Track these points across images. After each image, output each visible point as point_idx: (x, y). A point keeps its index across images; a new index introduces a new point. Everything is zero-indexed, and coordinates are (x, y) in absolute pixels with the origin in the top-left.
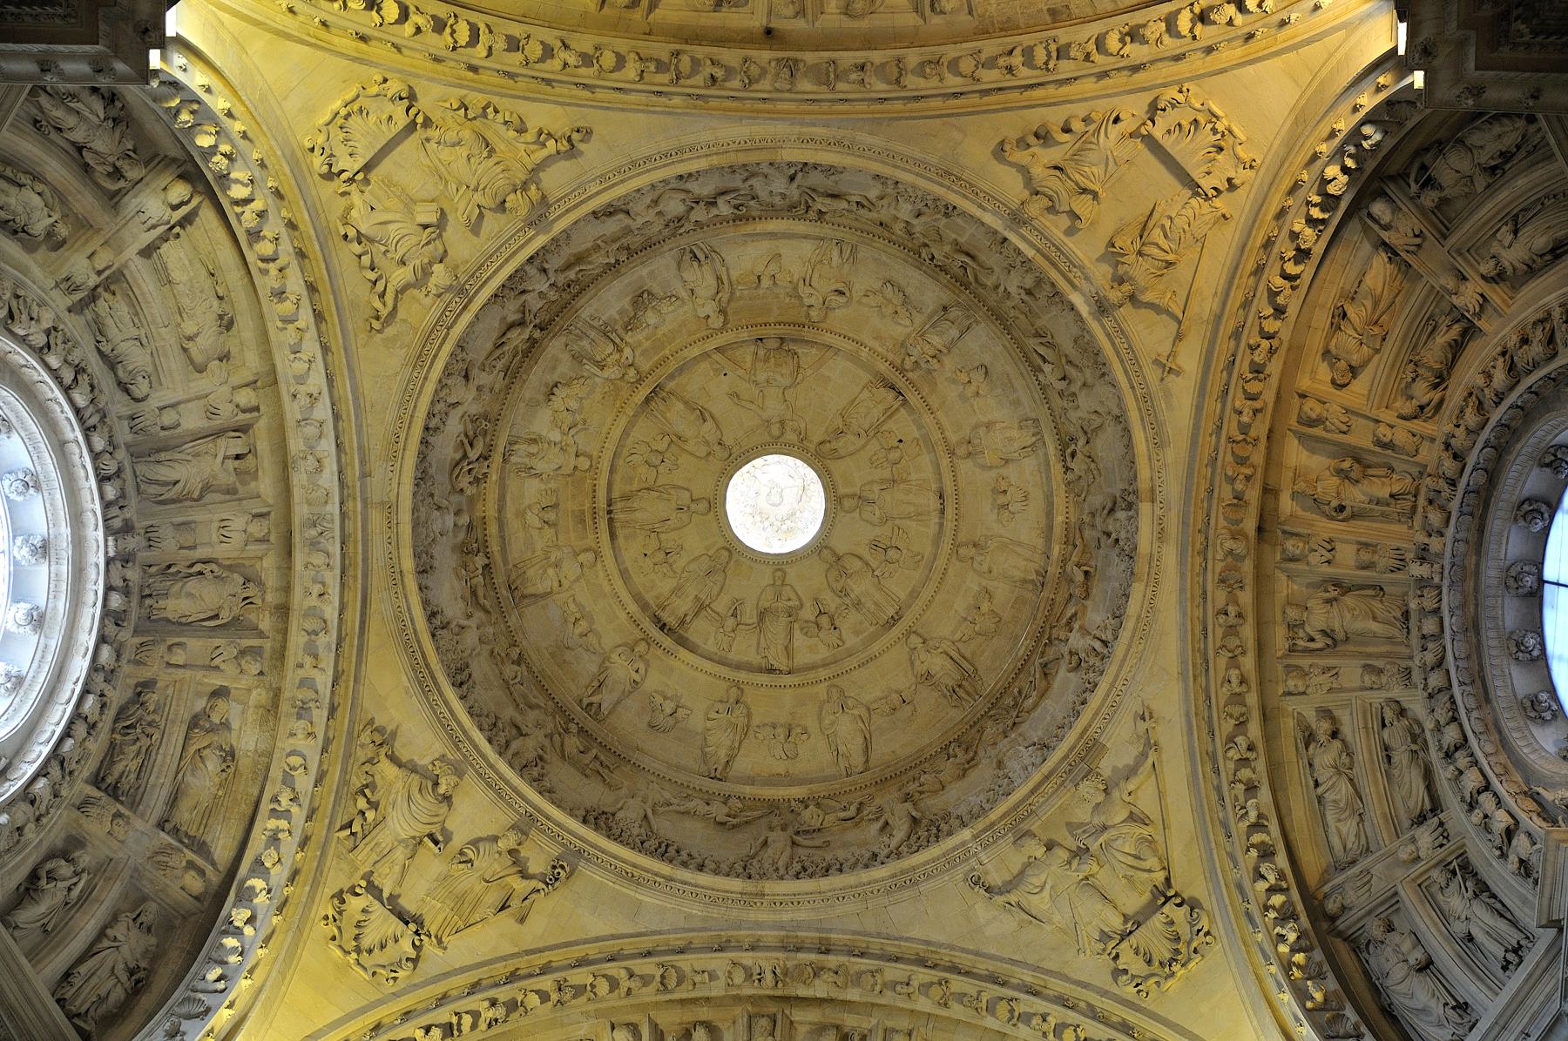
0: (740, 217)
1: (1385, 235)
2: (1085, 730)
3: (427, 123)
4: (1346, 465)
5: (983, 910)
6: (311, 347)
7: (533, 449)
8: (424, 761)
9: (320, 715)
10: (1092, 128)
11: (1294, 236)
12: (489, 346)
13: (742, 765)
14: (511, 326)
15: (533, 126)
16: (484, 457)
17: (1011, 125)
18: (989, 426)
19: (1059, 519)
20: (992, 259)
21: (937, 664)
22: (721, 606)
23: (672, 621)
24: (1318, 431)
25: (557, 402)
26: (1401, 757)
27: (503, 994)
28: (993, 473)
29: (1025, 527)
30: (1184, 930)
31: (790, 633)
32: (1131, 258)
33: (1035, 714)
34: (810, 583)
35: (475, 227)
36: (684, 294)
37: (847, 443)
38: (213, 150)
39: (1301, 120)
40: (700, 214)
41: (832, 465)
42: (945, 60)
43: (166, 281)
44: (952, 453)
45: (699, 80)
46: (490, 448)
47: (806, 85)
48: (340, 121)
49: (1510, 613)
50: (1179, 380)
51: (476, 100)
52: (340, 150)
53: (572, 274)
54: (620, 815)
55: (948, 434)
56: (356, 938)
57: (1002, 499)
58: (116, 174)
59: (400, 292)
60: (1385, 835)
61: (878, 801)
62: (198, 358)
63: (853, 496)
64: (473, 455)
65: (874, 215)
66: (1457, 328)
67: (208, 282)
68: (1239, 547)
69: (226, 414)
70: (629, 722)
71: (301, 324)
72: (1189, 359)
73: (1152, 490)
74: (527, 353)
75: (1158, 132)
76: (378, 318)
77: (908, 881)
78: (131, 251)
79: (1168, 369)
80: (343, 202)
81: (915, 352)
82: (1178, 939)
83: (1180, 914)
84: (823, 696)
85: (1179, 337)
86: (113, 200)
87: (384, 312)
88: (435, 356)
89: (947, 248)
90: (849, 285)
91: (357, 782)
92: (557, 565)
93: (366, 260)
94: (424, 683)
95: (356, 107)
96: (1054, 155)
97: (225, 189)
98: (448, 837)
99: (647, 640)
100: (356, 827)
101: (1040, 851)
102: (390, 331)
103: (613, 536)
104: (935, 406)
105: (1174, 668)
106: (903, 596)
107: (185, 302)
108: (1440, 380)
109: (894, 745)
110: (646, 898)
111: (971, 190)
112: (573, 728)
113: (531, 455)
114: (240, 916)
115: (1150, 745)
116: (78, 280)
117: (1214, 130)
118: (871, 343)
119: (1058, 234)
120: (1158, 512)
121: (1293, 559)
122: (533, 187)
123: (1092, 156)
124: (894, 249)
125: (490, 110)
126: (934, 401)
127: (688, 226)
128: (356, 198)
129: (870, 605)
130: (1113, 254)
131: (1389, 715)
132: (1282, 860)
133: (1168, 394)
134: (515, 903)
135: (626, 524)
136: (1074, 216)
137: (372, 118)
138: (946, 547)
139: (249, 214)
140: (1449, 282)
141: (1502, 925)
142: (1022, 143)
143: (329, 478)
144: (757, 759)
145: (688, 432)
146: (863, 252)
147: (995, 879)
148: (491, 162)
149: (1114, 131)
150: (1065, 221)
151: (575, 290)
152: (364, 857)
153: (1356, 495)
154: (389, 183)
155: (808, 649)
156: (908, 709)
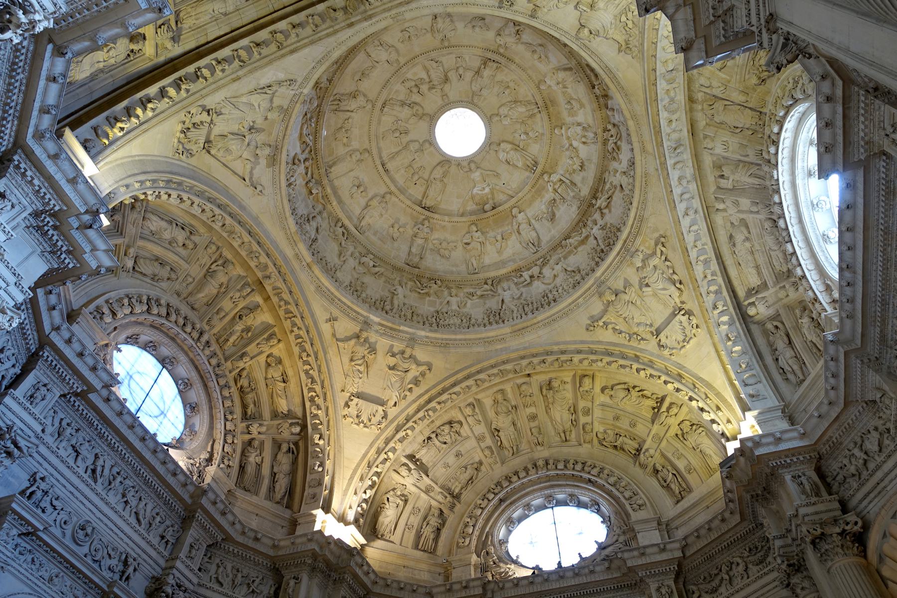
1: (290, 421)
3: (652, 333)
4: (250, 334)
5: (281, 76)
6: (689, 239)
10: (402, 395)
11: (319, 408)
12: (614, 198)
14: (607, 207)
15: (610, 331)
17: (431, 380)
19: (335, 203)
20: (413, 299)
21: (353, 105)
22: (469, 75)
23: (490, 64)
24: (265, 336)
28: (370, 195)
31: (429, 77)
32: (366, 352)
34: (431, 101)
35: (627, 284)
36: (533, 221)
37: (438, 172)
38: (735, 344)
39: (339, 448)
40: (535, 270)
41: (441, 158)
43: (757, 267)
48: (687, 340)
49: (165, 351)
50: (325, 318)
51: (634, 343)
52: (685, 324)
53: (585, 232)
55: (397, 200)
57: (362, 189)
58: (777, 327)
59: (654, 253)
62: (743, 229)
65: (465, 290)
66: (249, 413)
71: (695, 250)
72: (326, 328)
73: (310, 268)
74: (597, 191)
75: (380, 408)
76: (662, 243)
79: (332, 319)
80: (684, 298)
81: (426, 230)
85: (334, 335)
86: (776, 317)
87: (660, 246)
88: (635, 219)
89: (432, 291)
90: (465, 248)
96: (410, 376)
97: (731, 318)
99: (501, 54)
102: (656, 235)
106: (383, 118)
107: (750, 258)
108: (241, 390)
111: (434, 343)
113: (585, 136)
117: (363, 422)
120: (304, 263)
121: (245, 284)
123: (398, 385)
124: (452, 278)
126: (409, 210)
127: (539, 263)
128: (678, 301)
129: (398, 108)
130: (373, 350)
131: (173, 276)
133: (326, 310)
135: (529, 103)
136: (393, 355)
137: (674, 338)
138: (375, 152)
139: (721, 308)
140: (264, 429)
142: (423, 374)
143: (674, 175)
146: (463, 268)
147: (282, 90)
150: (396, 350)
151: (581, 222)
153: (239, 327)
154: (665, 305)
155: (417, 72)
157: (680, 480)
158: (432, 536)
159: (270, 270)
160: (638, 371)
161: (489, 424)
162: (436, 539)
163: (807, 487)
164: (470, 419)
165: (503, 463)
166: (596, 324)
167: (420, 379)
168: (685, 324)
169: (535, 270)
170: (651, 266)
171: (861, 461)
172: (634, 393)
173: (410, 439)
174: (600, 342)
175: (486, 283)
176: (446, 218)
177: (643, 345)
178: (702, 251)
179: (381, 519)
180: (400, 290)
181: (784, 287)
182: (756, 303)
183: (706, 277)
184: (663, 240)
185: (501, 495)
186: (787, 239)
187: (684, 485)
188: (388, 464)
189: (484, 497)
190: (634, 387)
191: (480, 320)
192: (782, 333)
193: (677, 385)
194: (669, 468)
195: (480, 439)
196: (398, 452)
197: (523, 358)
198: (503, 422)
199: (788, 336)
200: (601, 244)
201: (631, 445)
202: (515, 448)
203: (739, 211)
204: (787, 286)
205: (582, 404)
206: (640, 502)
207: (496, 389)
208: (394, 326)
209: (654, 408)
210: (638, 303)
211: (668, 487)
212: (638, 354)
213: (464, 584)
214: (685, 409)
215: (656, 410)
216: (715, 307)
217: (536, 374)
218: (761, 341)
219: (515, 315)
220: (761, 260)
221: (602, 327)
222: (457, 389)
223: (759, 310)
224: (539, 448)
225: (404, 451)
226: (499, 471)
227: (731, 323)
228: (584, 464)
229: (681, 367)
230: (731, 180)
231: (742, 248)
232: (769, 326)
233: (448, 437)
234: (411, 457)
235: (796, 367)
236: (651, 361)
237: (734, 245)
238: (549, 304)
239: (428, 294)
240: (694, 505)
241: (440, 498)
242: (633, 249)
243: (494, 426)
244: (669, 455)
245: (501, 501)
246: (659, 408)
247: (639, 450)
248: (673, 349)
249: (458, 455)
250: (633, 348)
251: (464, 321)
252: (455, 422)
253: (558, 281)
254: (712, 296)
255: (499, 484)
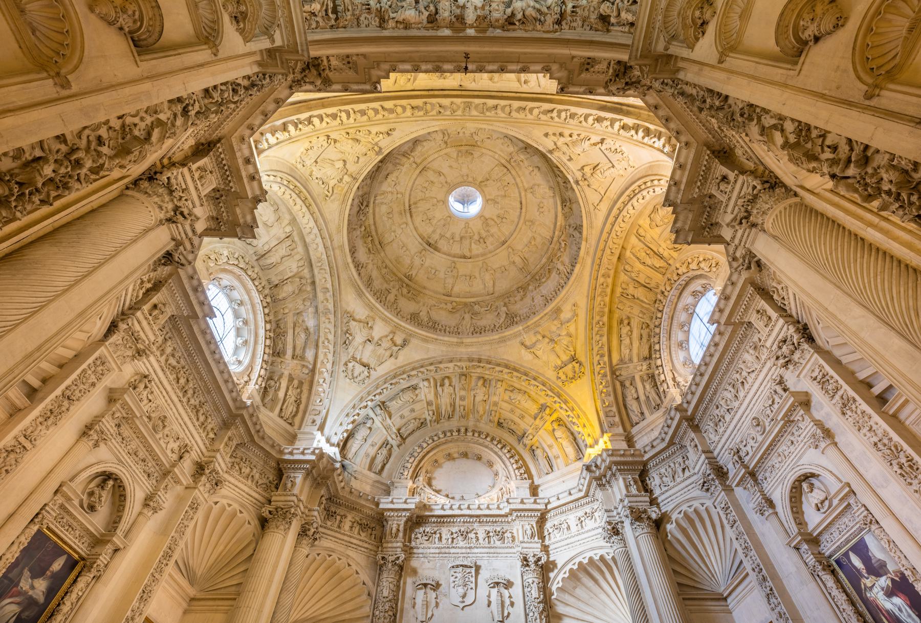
2: (558, 303)
5: (523, 351)
7: (383, 197)
8: (363, 318)
9: (332, 317)
13: (456, 289)
16: (367, 206)
18: (539, 185)
19: (558, 224)
21: (518, 260)
25: (389, 180)
26: (644, 340)
27: (394, 381)
29: (548, 219)
30: (577, 369)
33: (545, 284)
34: (477, 227)
42: (528, 108)
44: (526, 191)
45: (434, 113)
46: (368, 202)
47: (474, 113)
54: (421, 314)
55: (525, 184)
56: (352, 374)
60: (635, 359)
61: (497, 304)
63: (492, 200)
64: (363, 208)
68: (610, 267)
69: (284, 236)
70: (421, 277)
77: (503, 340)
82: (575, 372)
83: (577, 366)
84: (481, 265)
87: (329, 195)
91: (345, 329)
92: (394, 232)
94: (360, 294)
98: (373, 339)
100: (347, 342)
101: (541, 338)
103: (411, 216)
104: (521, 174)
105: (586, 294)
106: (507, 233)
109: (503, 285)
110: (431, 346)
112: (404, 285)
114: (321, 381)
115: (576, 315)
118: (499, 153)
132: (606, 359)
133: (596, 215)
134: (394, 354)
141: (657, 398)
143: (321, 248)
144: (460, 287)
145: (435, 180)
147: (528, 343)
149: (587, 143)
152: (351, 350)
156: (507, 273)
159: (603, 271)
167: (558, 134)
176: (497, 156)
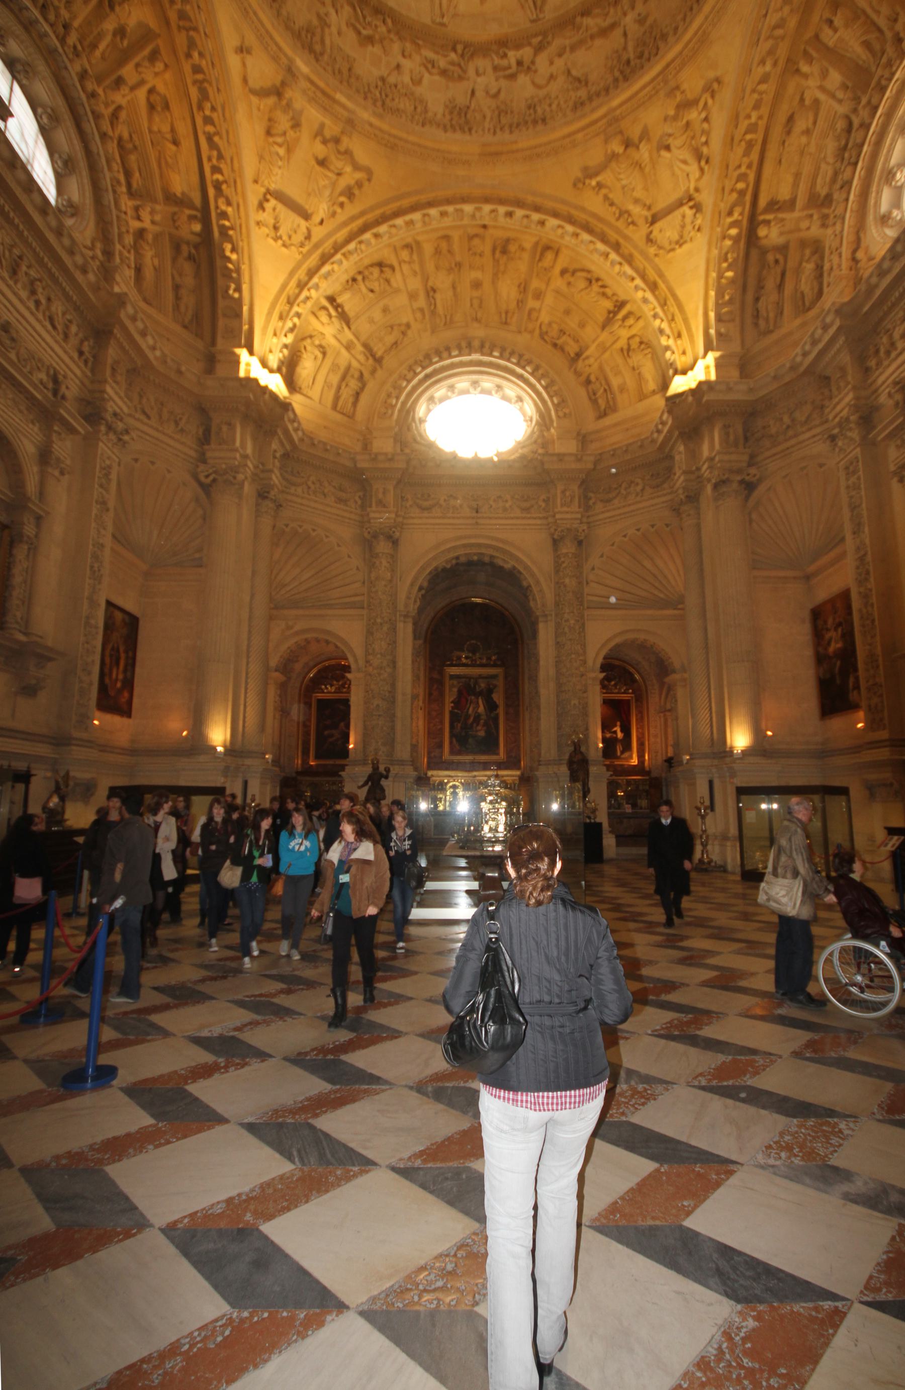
0: (503, 44)
3: (646, 218)
15: (601, 197)
17: (367, 199)
35: (645, 135)
38: (728, 269)
43: (797, 176)
48: (680, 243)
51: (620, 224)
58: (777, 261)
67: (783, 161)
78: (796, 214)
89: (377, 37)
93: (703, 139)
95: (673, 246)
97: (739, 235)
102: (711, 74)
116: (819, 223)
119: (328, 122)
122: (609, 151)
125: (617, 215)
127: (535, 41)
137: (668, 234)
139: (736, 216)
148: (624, 182)
157: (609, 396)
158: (351, 400)
160: (613, 263)
161: (426, 279)
162: (355, 403)
163: (732, 437)
164: (405, 267)
165: (433, 332)
166: (587, 181)
168: (688, 220)
169: (526, 53)
170: (684, 121)
171: (784, 426)
172: (595, 288)
173: (334, 277)
174: (583, 209)
175: (454, 49)
177: (630, 231)
178: (752, 128)
179: (299, 370)
180: (333, 18)
181: (811, 216)
182: (773, 224)
183: (739, 166)
184: (715, 86)
185: (429, 370)
186: (853, 160)
187: (611, 403)
188: (309, 304)
189: (410, 369)
190: (598, 280)
191: (439, 116)
192: (779, 270)
193: (649, 295)
194: (603, 382)
195: (413, 296)
196: (321, 291)
197: (487, 200)
198: (442, 281)
199: (783, 274)
200: (630, 48)
201: (572, 348)
202: (448, 318)
203: (822, 88)
204: (815, 217)
205: (535, 284)
206: (567, 411)
207: (441, 233)
208: (328, 90)
209: (609, 312)
210: (647, 170)
211: (594, 402)
212: (621, 241)
213: (390, 456)
214: (641, 323)
215: (611, 315)
216: (730, 213)
217: (495, 227)
218: (753, 271)
219: (487, 125)
220: (807, 170)
221: (594, 188)
222: (399, 221)
223: (770, 235)
224: (476, 325)
225: (325, 290)
226: (427, 341)
227: (736, 240)
228: (521, 356)
229: (661, 275)
230: (838, 34)
231: (797, 140)
232: (770, 257)
233: (376, 284)
234: (331, 299)
235: (772, 315)
236: (631, 255)
237: (789, 133)
238: (535, 122)
239: (370, 40)
240: (616, 425)
241: (361, 358)
242: (672, 84)
243: (430, 284)
244: (607, 369)
245: (428, 377)
246: (615, 313)
247: (578, 355)
248: (660, 248)
249: (385, 310)
250: (618, 231)
251: (419, 110)
252: (387, 266)
253: (554, 88)
254: (735, 195)
255: (428, 356)
